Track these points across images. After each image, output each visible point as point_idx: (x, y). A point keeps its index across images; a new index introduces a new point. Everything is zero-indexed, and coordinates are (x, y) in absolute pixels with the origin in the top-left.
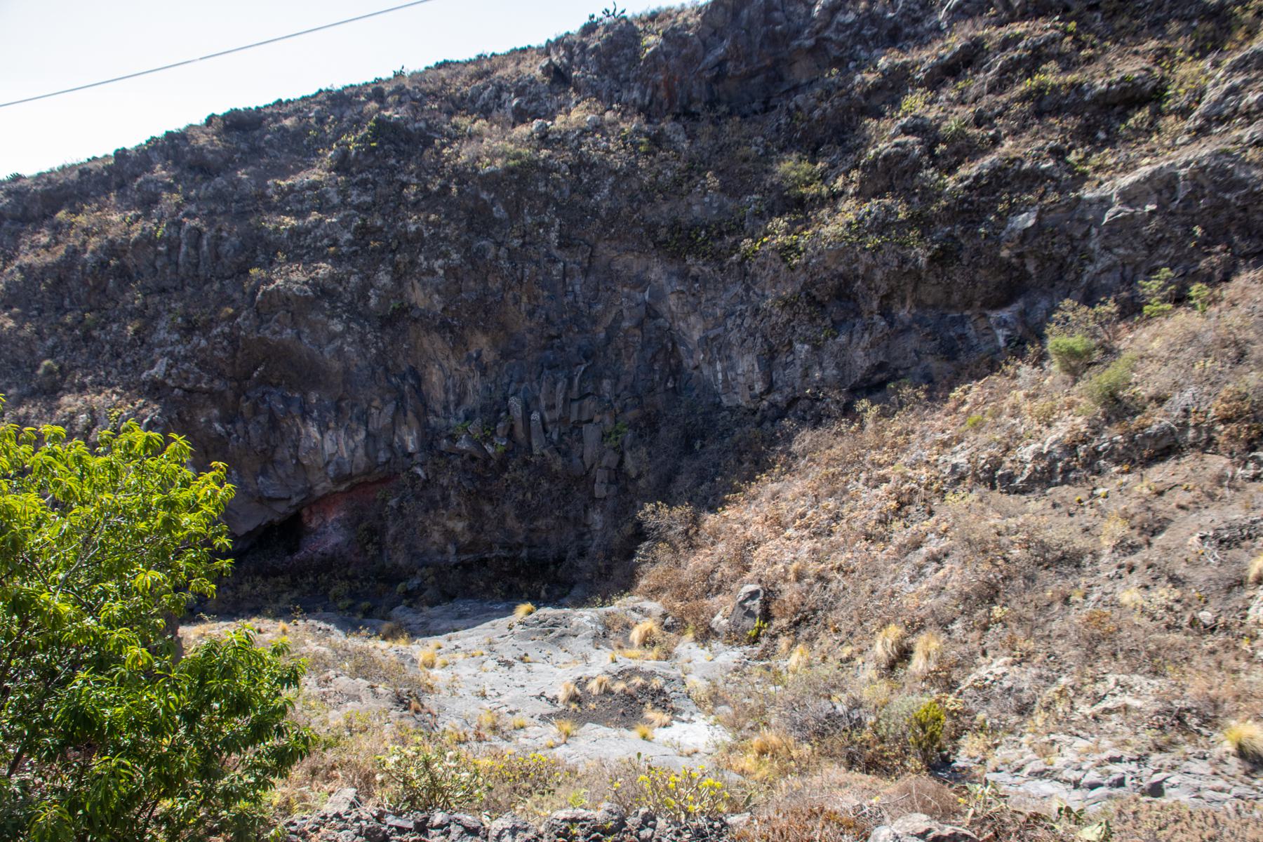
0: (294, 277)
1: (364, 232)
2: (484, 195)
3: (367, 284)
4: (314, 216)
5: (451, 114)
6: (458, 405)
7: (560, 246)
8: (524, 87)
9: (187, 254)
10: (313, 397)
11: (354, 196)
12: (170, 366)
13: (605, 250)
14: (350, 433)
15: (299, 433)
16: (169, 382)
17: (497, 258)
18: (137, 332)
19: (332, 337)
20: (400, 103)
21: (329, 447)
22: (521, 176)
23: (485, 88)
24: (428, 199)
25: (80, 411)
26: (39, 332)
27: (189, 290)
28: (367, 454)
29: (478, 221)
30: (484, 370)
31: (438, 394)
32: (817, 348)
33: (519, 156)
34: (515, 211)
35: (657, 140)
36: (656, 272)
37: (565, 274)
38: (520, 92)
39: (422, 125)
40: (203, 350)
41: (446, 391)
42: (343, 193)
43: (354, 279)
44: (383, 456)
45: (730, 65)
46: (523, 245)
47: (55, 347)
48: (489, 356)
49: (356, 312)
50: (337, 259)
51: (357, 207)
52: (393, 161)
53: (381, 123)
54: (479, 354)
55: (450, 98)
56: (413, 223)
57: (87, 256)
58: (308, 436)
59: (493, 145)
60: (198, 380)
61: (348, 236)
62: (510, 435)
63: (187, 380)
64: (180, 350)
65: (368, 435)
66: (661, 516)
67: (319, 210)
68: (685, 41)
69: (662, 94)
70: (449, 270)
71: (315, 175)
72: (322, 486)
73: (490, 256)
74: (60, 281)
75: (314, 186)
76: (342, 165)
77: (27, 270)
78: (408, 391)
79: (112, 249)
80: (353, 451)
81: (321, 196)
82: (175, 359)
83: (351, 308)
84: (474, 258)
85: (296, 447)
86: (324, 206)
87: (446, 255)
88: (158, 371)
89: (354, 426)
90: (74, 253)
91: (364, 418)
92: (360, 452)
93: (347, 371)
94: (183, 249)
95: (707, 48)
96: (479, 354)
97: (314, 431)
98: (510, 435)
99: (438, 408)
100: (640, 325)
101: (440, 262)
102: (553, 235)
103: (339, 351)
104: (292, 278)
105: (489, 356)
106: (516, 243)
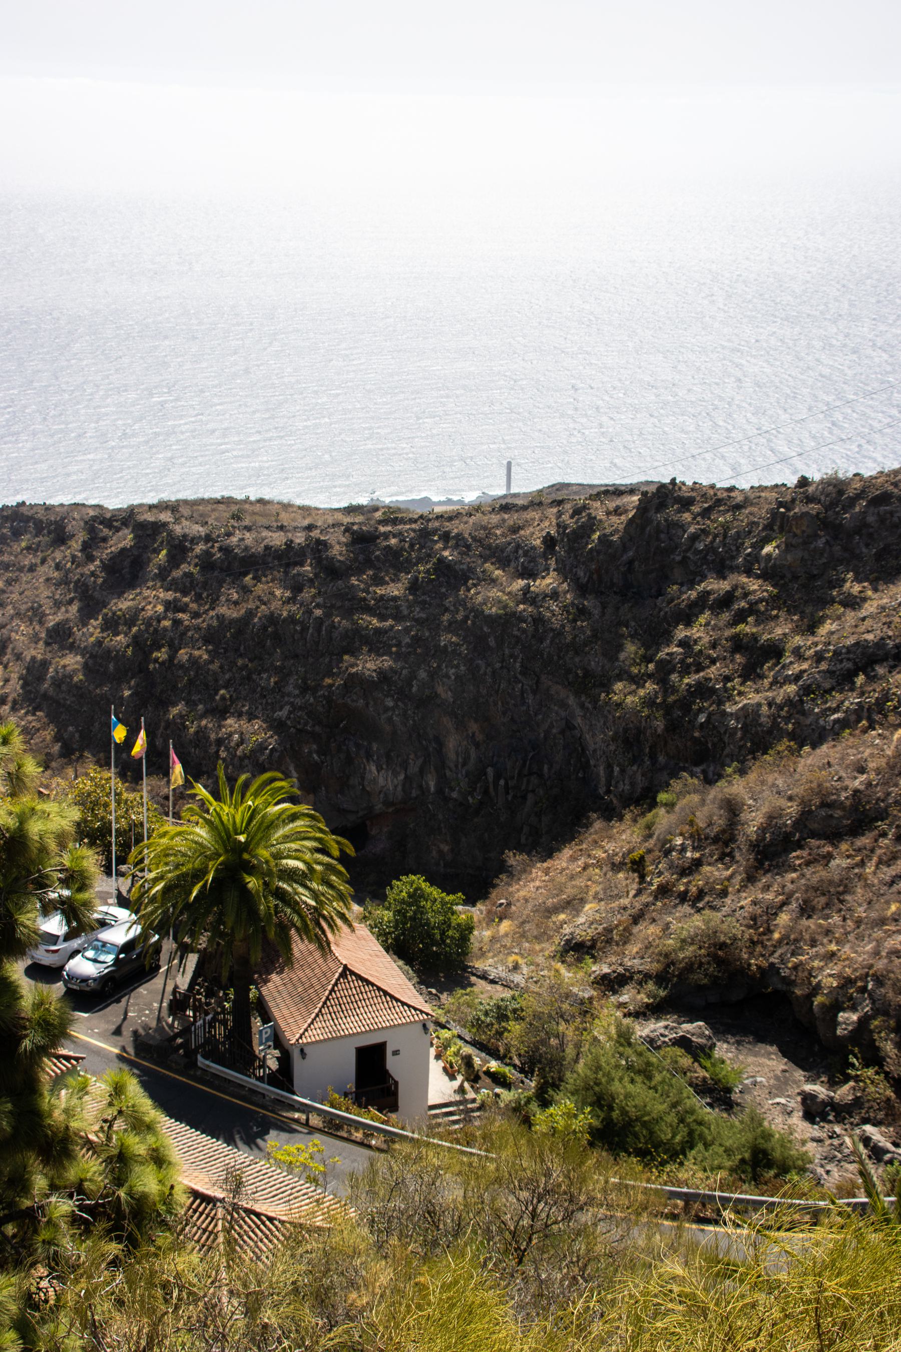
0: (368, 665)
1: (417, 640)
2: (485, 629)
3: (413, 676)
4: (390, 622)
6: (464, 765)
7: (520, 673)
8: (528, 551)
9: (312, 635)
10: (375, 747)
11: (418, 613)
12: (290, 712)
14: (395, 774)
15: (365, 769)
16: (289, 722)
17: (485, 674)
18: (276, 683)
19: (387, 709)
20: (457, 546)
21: (381, 781)
22: (508, 619)
23: (509, 544)
24: (452, 627)
25: (235, 732)
26: (221, 667)
27: (311, 660)
28: (403, 790)
30: (477, 745)
31: (452, 756)
32: (623, 771)
33: (505, 607)
35: (582, 612)
36: (571, 701)
37: (522, 692)
38: (526, 554)
39: (465, 567)
40: (311, 705)
41: (457, 754)
43: (405, 672)
44: (414, 794)
45: (636, 563)
46: (502, 667)
47: (229, 680)
48: (480, 737)
50: (398, 657)
51: (416, 620)
52: (443, 590)
53: (441, 560)
54: (473, 734)
55: (489, 547)
56: (446, 639)
57: (256, 620)
58: (370, 771)
59: (497, 592)
60: (306, 724)
61: (408, 640)
62: (486, 792)
63: (299, 723)
64: (298, 702)
65: (406, 777)
66: (513, 859)
67: (394, 619)
69: (595, 576)
70: (458, 677)
71: (395, 590)
73: (482, 672)
74: (240, 632)
75: (395, 599)
76: (414, 587)
77: (220, 618)
79: (272, 619)
80: (396, 787)
81: (397, 608)
82: (294, 708)
85: (363, 778)
86: (398, 618)
87: (457, 667)
88: (283, 714)
89: (398, 769)
90: (250, 614)
91: (405, 765)
92: (400, 788)
94: (311, 631)
95: (625, 549)
96: (473, 734)
97: (374, 768)
98: (486, 792)
99: (452, 765)
100: (562, 732)
101: (453, 671)
102: (518, 665)
103: (390, 720)
104: (368, 665)
105: (480, 737)
106: (498, 665)
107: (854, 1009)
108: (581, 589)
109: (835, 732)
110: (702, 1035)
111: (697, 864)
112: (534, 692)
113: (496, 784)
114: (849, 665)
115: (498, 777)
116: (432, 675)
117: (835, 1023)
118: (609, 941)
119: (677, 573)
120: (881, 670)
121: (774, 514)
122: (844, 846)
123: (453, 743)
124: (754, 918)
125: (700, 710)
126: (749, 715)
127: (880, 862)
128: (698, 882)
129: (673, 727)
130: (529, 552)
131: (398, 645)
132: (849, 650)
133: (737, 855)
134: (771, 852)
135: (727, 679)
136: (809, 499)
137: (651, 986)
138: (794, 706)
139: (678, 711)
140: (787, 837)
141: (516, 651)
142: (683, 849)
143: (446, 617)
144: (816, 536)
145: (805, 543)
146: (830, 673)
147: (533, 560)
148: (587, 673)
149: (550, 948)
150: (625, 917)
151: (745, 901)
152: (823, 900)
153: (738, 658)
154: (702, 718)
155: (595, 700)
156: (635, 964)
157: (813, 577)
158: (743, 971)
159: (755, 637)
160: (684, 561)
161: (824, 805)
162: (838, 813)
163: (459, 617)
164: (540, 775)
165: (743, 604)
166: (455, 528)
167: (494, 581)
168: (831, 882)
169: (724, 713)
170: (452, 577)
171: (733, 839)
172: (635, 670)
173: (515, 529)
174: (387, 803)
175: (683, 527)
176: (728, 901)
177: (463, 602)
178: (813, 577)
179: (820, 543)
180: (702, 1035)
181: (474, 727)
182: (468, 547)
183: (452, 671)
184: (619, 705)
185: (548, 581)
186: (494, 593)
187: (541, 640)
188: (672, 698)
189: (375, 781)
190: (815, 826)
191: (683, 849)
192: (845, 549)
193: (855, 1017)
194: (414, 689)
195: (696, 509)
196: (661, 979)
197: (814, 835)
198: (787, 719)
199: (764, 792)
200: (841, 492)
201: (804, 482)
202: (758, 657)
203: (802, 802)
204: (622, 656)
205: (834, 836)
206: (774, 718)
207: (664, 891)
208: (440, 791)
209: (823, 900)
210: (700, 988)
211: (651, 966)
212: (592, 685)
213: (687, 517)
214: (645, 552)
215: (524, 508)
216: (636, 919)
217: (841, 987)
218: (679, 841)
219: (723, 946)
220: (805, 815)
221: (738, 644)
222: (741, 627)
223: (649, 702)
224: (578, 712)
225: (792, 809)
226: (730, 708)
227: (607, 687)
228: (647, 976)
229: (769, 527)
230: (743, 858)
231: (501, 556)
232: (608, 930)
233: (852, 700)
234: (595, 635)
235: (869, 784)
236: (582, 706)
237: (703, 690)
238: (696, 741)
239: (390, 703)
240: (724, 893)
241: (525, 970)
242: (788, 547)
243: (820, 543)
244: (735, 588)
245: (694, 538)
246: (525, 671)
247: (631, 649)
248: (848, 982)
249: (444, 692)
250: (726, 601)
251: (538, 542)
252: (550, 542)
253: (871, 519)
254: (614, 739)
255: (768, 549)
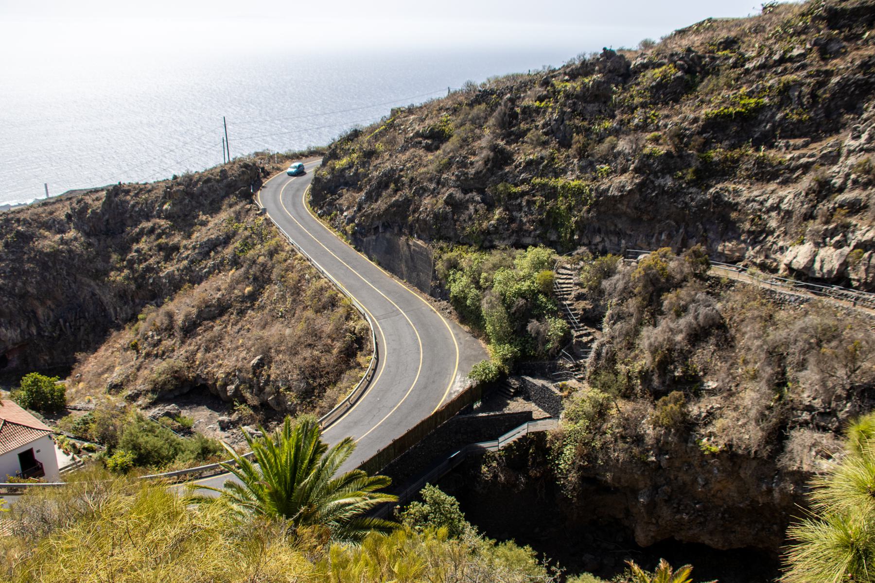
1: (13, 269)
3: (15, 285)
5: (40, 228)
11: (11, 256)
13: (79, 277)
14: (15, 330)
19: (5, 302)
20: (24, 224)
21: (9, 335)
22: (55, 254)
24: (30, 260)
29: (44, 266)
30: (53, 310)
31: (41, 317)
32: (121, 309)
33: (53, 248)
34: (54, 264)
36: (92, 283)
38: (59, 223)
42: (7, 254)
44: (27, 337)
48: (53, 307)
49: (11, 294)
51: (12, 260)
53: (18, 232)
55: (40, 222)
56: (27, 266)
59: (49, 241)
62: (61, 330)
65: (21, 331)
66: (79, 356)
68: (97, 213)
70: (37, 282)
72: (10, 347)
78: (32, 317)
83: (10, 293)
84: (44, 278)
91: (19, 325)
93: (11, 312)
95: (104, 214)
98: (61, 330)
100: (91, 297)
103: (7, 307)
105: (53, 307)
107: (232, 384)
108: (87, 235)
109: (206, 276)
110: (175, 409)
111: (160, 341)
112: (75, 283)
113: (65, 325)
114: (207, 249)
115: (65, 322)
116: (24, 283)
117: (226, 391)
118: (129, 381)
119: (129, 222)
120: (219, 249)
121: (165, 192)
122: (218, 321)
123: (40, 312)
124: (187, 358)
125: (150, 278)
126: (170, 276)
127: (233, 325)
128: (161, 348)
129: (139, 287)
130: (60, 222)
131: (5, 273)
132: (205, 243)
133: (176, 334)
134: (189, 330)
135: (158, 263)
136: (179, 184)
137: (150, 395)
138: (188, 269)
139: (140, 280)
140: (194, 322)
141: (63, 266)
142: (153, 336)
143: (26, 257)
144: (184, 199)
145: (181, 202)
146: (200, 253)
147: (62, 225)
148: (97, 271)
149: (104, 390)
150: (134, 369)
151: (182, 352)
152: (213, 344)
153: (161, 253)
154: (151, 281)
155: (103, 282)
156: (142, 387)
157: (186, 215)
158: (186, 380)
159: (167, 244)
160: (131, 216)
161: (207, 307)
162: (213, 309)
163: (32, 255)
164: (85, 317)
165: (159, 231)
166: (22, 216)
167: (45, 237)
168: (215, 337)
169: (160, 277)
170: (25, 238)
171: (172, 328)
172: (118, 266)
173: (51, 213)
174: (14, 344)
175: (128, 203)
176: (175, 353)
177: (33, 249)
178: (186, 215)
179: (187, 201)
180: (175, 409)
181: (49, 303)
182: (30, 224)
183: (33, 280)
184: (114, 281)
185: (71, 233)
186: (47, 242)
187: (73, 260)
188: (136, 275)
189: (5, 335)
190: (205, 316)
191: (153, 336)
192: (197, 203)
193: (233, 387)
194: (17, 291)
195: (132, 194)
196: (153, 391)
197: (205, 319)
198: (186, 275)
199: (182, 306)
200: (191, 180)
201: (175, 177)
202: (169, 252)
203: (199, 307)
204: (111, 261)
205: (213, 318)
206: (181, 275)
207: (148, 355)
208: (39, 334)
209: (213, 344)
210: (171, 391)
211: (150, 387)
212: (100, 275)
213: (128, 198)
214: (112, 216)
215: (54, 203)
216: (138, 369)
217: (226, 377)
218: (150, 333)
219: (176, 372)
220: (200, 312)
221: (160, 248)
222: (160, 240)
223: (127, 278)
224: (97, 288)
225: (195, 311)
226: (162, 274)
227: (107, 274)
228: (147, 391)
229: (164, 197)
230: (178, 335)
231: (47, 226)
232: (128, 376)
233: (211, 263)
234: (97, 254)
235: (223, 295)
236: (98, 285)
237: (149, 269)
238: (150, 291)
239: (6, 299)
240: (173, 350)
241: (94, 402)
242: (174, 205)
243: (187, 201)
244: (155, 224)
245: (134, 206)
246: (68, 274)
247: (115, 257)
248: (228, 374)
249: (31, 290)
250: (152, 231)
251: (63, 217)
252: (69, 217)
253: (205, 189)
254: (115, 296)
255: (165, 207)
